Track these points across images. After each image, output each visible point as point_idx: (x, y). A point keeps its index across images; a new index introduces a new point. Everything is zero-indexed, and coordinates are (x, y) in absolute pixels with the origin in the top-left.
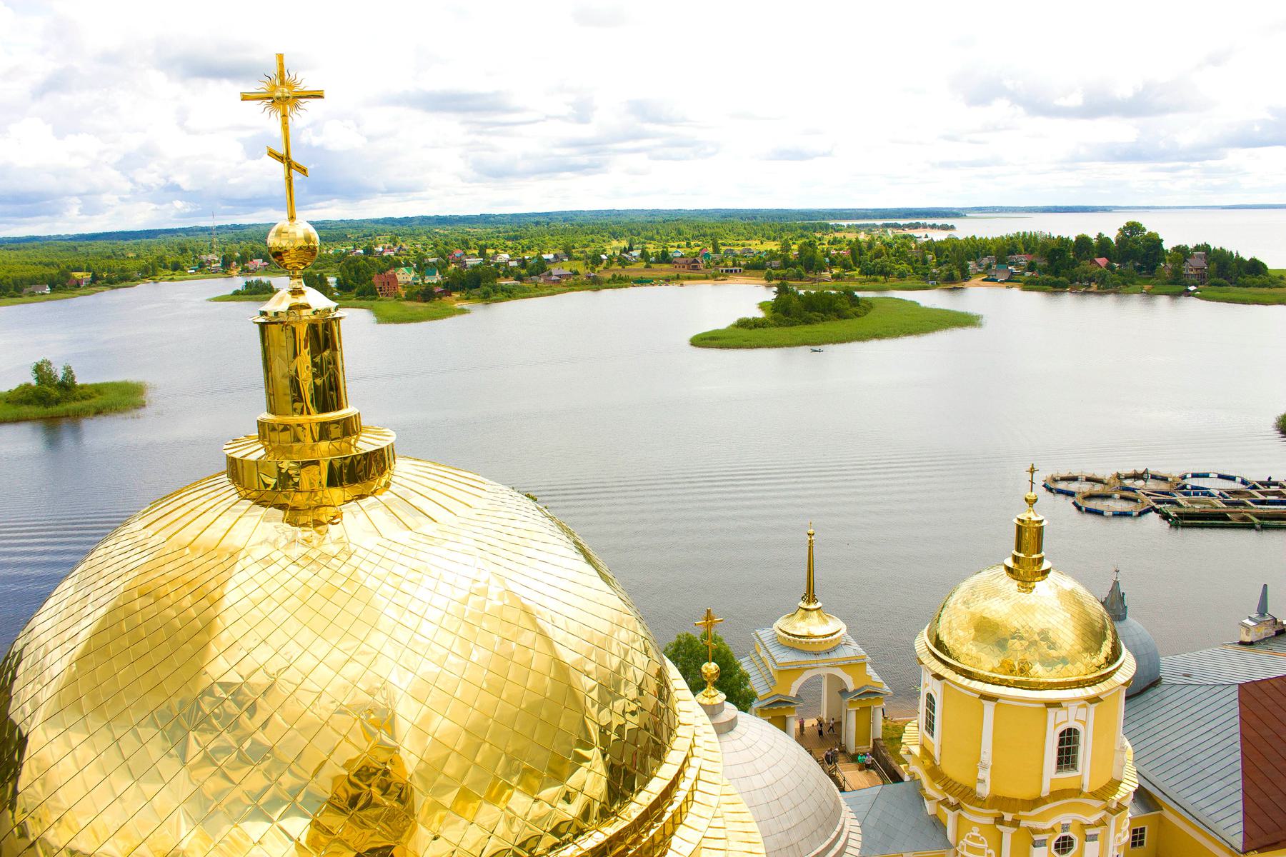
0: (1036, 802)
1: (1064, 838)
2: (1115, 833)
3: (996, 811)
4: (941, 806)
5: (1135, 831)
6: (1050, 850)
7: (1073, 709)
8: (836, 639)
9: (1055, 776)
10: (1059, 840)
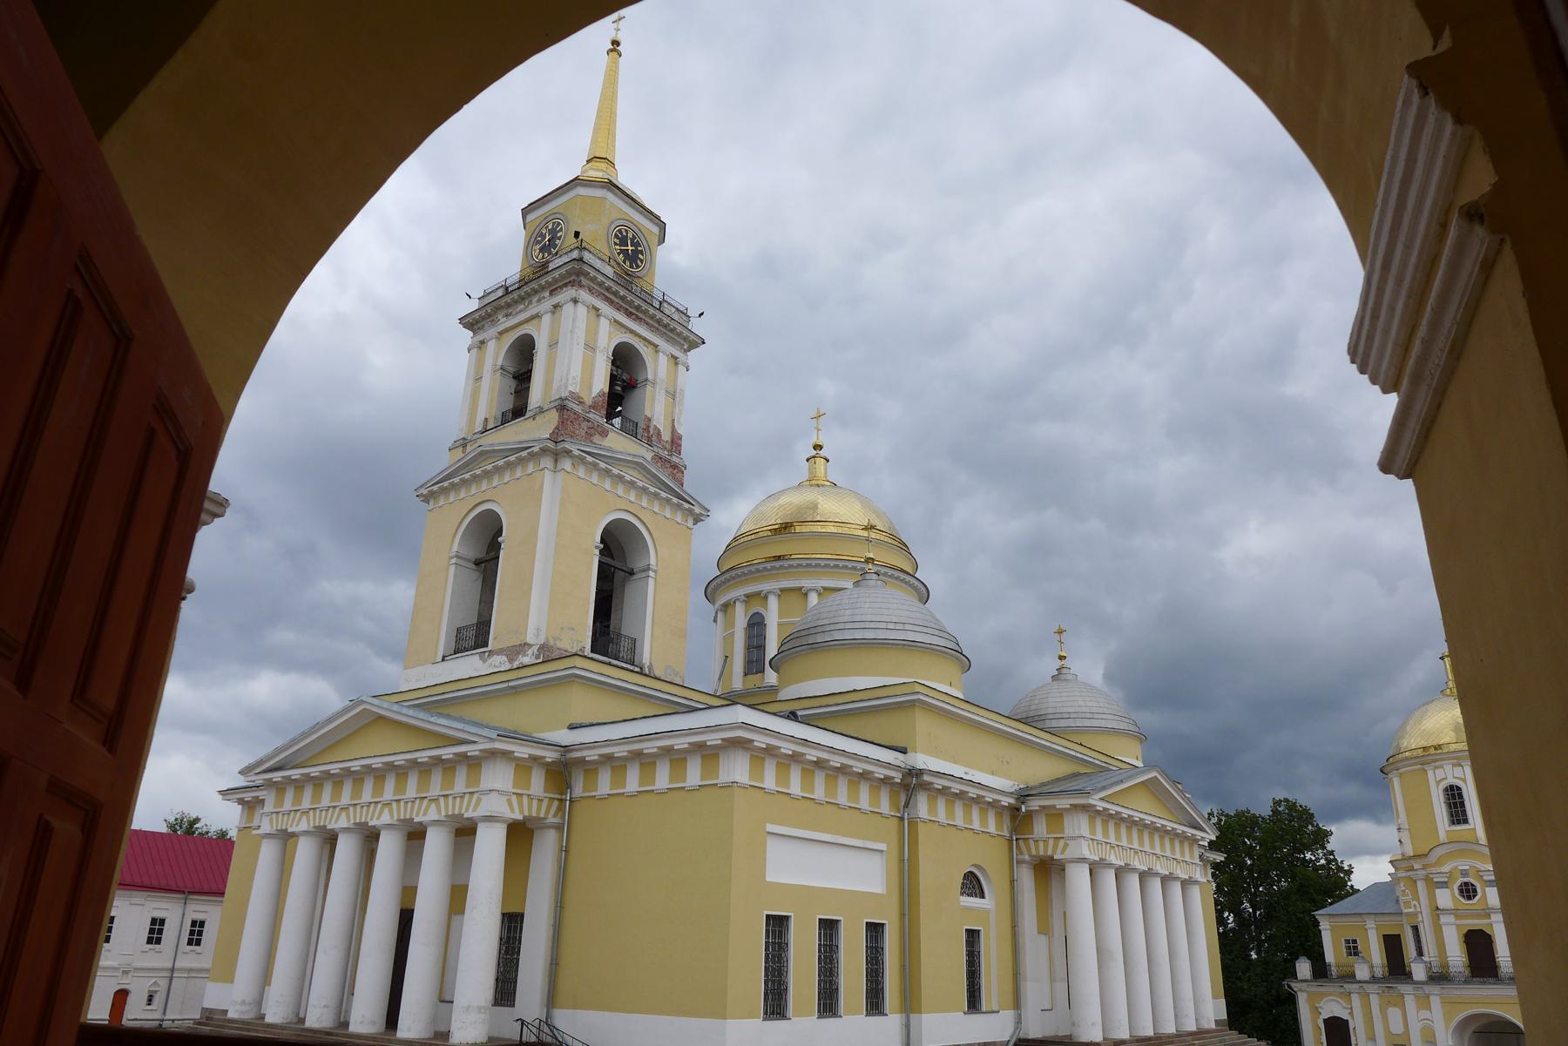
6: (1453, 895)
9: (1448, 829)
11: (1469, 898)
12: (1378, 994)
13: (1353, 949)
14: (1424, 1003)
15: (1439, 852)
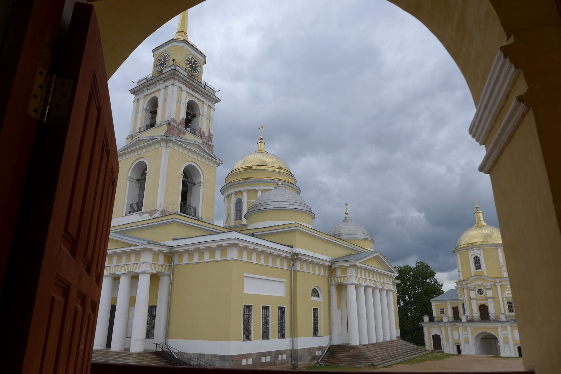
11: (481, 294)
12: (450, 326)
13: (442, 312)
14: (465, 329)
15: (472, 279)
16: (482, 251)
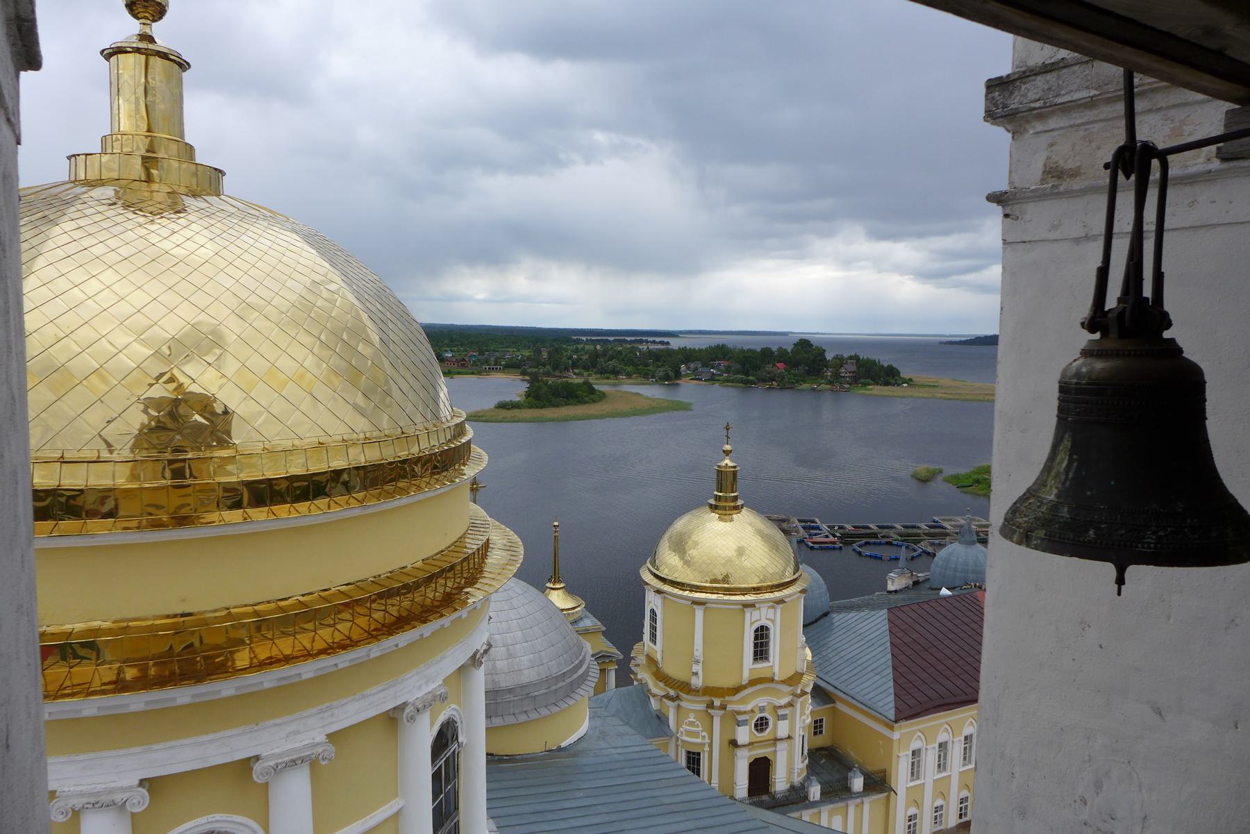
0: (737, 689)
1: (762, 719)
2: (800, 717)
3: (707, 698)
4: (664, 700)
5: (816, 722)
7: (764, 610)
8: (576, 612)
10: (757, 721)
11: (762, 730)
16: (779, 611)
